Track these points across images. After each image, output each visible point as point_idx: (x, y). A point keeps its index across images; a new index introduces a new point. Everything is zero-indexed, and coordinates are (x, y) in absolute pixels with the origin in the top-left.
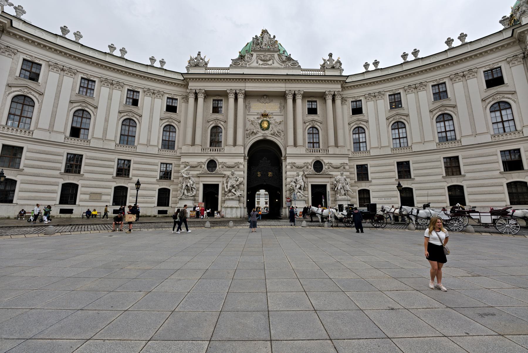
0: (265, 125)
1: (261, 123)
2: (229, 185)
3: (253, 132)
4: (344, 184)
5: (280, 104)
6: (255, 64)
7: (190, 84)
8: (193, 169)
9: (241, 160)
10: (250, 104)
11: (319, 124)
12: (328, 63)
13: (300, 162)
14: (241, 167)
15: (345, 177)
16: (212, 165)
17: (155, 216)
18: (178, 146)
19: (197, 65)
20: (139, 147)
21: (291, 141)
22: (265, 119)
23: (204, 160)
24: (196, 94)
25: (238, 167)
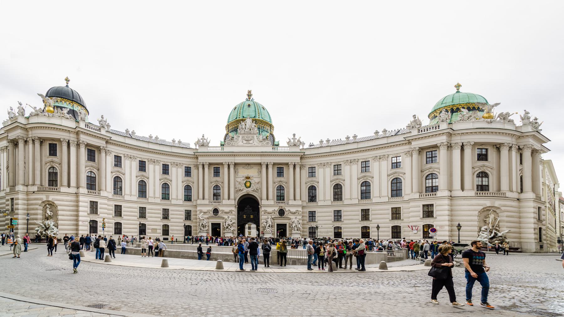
0: (248, 184)
2: (227, 224)
6: (241, 144)
7: (199, 158)
13: (270, 210)
14: (234, 213)
16: (216, 211)
19: (203, 145)
21: (264, 196)
23: (211, 208)
24: (203, 165)
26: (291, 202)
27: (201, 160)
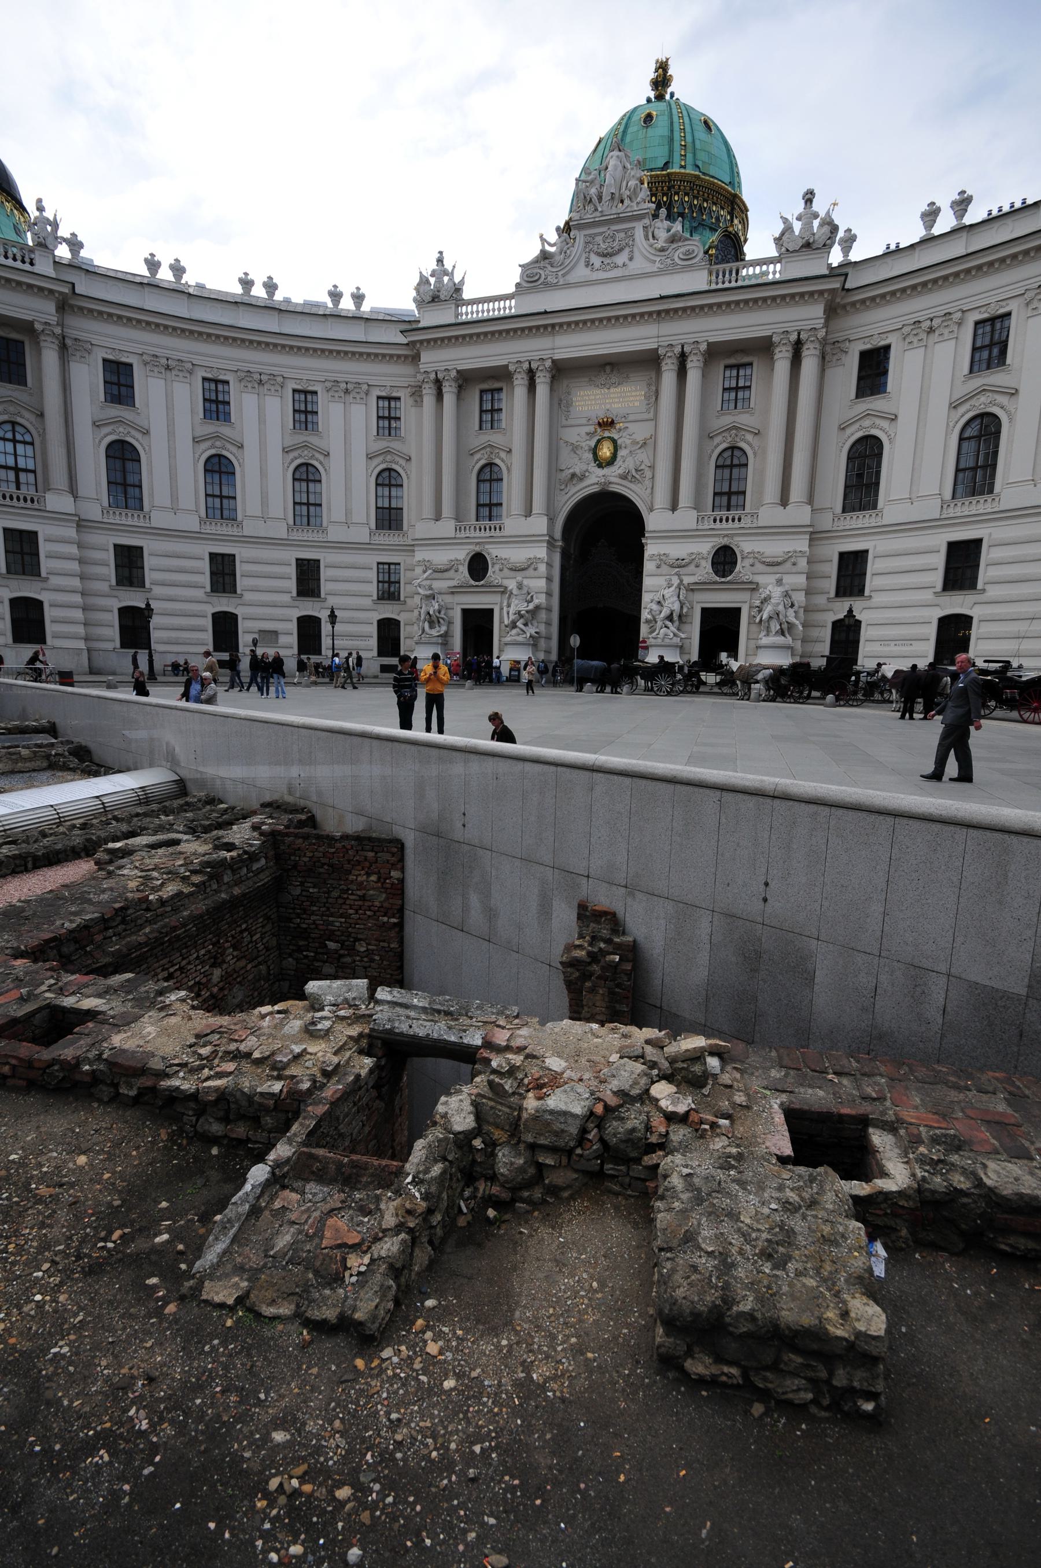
0: (606, 451)
1: (596, 446)
2: (512, 610)
3: (573, 475)
4: (781, 608)
5: (649, 385)
8: (439, 575)
9: (541, 552)
10: (569, 393)
11: (749, 437)
12: (797, 227)
13: (678, 550)
15: (787, 587)
16: (478, 566)
17: (376, 677)
18: (409, 523)
19: (435, 299)
20: (331, 529)
21: (662, 497)
22: (607, 434)
24: (438, 383)
25: (535, 569)
26: (770, 514)
27: (432, 360)
